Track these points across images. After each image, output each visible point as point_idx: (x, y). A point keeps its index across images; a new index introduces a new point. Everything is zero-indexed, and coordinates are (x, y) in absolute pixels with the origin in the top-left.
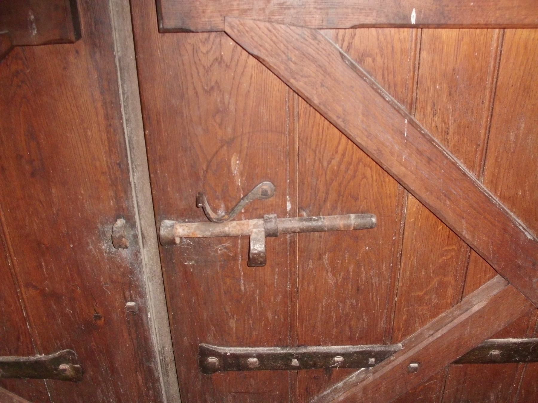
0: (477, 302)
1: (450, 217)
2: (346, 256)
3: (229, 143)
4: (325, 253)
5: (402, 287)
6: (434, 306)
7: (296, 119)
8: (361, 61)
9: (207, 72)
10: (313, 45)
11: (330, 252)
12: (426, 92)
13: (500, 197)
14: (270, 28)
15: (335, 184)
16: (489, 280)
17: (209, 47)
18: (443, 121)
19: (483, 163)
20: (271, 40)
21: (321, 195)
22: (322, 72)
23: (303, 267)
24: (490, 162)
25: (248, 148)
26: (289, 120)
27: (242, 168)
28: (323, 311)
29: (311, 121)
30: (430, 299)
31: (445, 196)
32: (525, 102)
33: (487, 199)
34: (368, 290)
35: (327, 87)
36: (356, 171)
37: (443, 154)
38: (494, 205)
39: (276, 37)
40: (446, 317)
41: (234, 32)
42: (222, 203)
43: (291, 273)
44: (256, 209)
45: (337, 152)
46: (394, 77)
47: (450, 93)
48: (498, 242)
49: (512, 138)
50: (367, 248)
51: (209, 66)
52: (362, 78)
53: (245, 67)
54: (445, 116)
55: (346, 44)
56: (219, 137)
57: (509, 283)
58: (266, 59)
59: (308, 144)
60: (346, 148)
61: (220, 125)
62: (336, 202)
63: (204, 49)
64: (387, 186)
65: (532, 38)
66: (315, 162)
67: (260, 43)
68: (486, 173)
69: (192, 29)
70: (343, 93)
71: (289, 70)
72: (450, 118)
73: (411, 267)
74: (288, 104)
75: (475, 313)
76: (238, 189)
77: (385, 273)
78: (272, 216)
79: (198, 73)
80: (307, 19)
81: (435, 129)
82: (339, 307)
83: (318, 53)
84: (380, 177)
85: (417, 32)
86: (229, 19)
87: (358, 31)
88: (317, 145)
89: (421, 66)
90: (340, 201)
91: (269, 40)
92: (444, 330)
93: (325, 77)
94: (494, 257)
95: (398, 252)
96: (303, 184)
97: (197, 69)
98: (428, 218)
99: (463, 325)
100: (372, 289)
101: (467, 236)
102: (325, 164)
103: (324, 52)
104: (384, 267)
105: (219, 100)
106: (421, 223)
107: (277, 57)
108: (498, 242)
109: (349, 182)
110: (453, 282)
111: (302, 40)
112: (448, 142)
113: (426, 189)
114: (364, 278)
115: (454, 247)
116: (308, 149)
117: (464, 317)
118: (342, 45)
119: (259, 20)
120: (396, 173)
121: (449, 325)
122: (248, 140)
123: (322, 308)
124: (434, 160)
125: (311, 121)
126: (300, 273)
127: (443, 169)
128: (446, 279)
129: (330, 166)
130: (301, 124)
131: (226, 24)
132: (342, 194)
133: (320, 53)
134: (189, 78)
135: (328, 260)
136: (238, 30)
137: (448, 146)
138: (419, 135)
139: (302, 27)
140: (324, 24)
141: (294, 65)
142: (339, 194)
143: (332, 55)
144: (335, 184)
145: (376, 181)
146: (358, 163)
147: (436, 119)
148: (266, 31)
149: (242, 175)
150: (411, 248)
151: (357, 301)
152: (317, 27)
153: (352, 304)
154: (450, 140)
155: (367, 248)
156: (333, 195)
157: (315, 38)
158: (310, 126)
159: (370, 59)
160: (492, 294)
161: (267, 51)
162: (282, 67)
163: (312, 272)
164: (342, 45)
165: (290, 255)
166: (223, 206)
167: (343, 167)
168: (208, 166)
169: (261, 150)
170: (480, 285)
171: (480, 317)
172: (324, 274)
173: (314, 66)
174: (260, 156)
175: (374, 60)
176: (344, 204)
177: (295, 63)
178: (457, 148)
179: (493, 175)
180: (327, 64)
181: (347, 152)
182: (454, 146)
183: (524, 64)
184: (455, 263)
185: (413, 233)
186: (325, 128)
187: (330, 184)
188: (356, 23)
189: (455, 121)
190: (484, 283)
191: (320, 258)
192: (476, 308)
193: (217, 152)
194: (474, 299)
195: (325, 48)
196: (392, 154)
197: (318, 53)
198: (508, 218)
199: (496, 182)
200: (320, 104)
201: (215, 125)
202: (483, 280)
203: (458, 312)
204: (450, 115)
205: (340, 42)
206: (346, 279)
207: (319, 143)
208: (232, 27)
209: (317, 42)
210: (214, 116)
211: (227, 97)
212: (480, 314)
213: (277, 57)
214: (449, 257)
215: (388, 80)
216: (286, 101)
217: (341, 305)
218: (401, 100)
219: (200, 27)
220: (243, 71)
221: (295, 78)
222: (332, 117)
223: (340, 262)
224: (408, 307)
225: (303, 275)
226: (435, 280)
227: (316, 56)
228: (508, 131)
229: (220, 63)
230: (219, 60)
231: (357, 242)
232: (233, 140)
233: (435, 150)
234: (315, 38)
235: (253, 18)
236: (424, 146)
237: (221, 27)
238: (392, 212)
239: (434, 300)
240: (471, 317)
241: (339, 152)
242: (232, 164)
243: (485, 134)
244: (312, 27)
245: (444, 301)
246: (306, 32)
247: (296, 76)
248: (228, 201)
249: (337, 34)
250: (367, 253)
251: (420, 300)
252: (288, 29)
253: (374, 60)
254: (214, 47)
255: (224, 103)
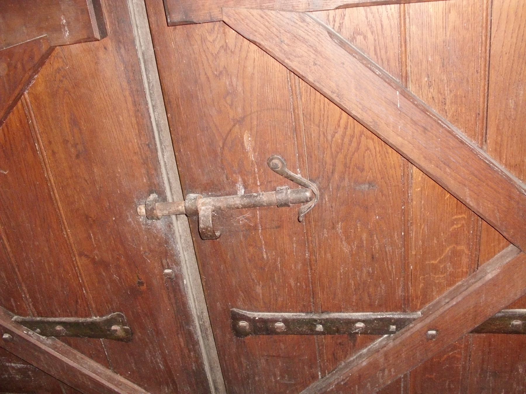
0: (491, 271)
1: (452, 184)
2: (358, 225)
3: (240, 121)
4: (338, 222)
5: (416, 255)
6: (450, 275)
7: (299, 97)
8: (353, 39)
9: (215, 58)
10: (302, 27)
11: (342, 221)
12: (420, 65)
13: (506, 165)
14: (263, 15)
15: (341, 156)
16: (503, 248)
17: (215, 37)
18: (439, 92)
19: (485, 131)
20: (265, 25)
21: (329, 167)
22: (314, 52)
23: (318, 237)
24: (492, 131)
25: (257, 125)
26: (293, 98)
27: (254, 145)
28: (341, 278)
29: (312, 98)
30: (445, 267)
31: (444, 164)
32: (522, 69)
33: (489, 166)
34: (383, 258)
35: (319, 65)
36: (359, 143)
37: (438, 123)
38: (496, 172)
39: (268, 22)
40: (462, 285)
41: (231, 20)
42: (240, 177)
43: (308, 242)
44: (270, 182)
45: (339, 126)
46: (386, 52)
47: (443, 64)
48: (504, 209)
49: (512, 105)
50: (377, 217)
51: (216, 53)
52: (351, 54)
53: (248, 52)
54: (440, 87)
55: (337, 25)
56: (231, 117)
57: (521, 251)
58: (262, 43)
59: (312, 119)
60: (348, 122)
61: (231, 105)
62: (344, 173)
63: (210, 39)
64: (390, 156)
65: (522, 5)
66: (320, 136)
67: (254, 29)
68: (488, 141)
69: (195, 21)
70: (335, 70)
71: (283, 51)
72: (446, 88)
73: (422, 236)
74: (290, 83)
75: (488, 281)
76: (252, 164)
77: (397, 241)
78: (284, 187)
79: (208, 60)
80: (294, 3)
81: (431, 100)
82: (356, 274)
83: (308, 35)
84: (382, 148)
85: (400, 8)
86: (225, 9)
87: (348, 10)
88: (320, 120)
89: (411, 40)
90: (347, 173)
91: (262, 26)
92: (460, 298)
93: (316, 55)
94: (501, 224)
95: (408, 221)
96: (311, 157)
97: (206, 56)
98: (434, 187)
99: (478, 292)
100: (387, 257)
101: (471, 204)
102: (329, 138)
103: (313, 33)
104: (396, 236)
105: (228, 83)
106: (428, 192)
107: (271, 40)
108: (504, 209)
109: (354, 154)
110: (466, 251)
111: (292, 23)
112: (446, 112)
113: (425, 157)
114: (377, 247)
115: (464, 215)
116: (312, 124)
117: (478, 285)
118: (334, 25)
119: (252, 8)
120: (393, 143)
121: (463, 293)
122: (257, 118)
123: (341, 275)
124: (429, 129)
125: (312, 98)
126: (317, 241)
127: (440, 138)
128: (458, 248)
129: (334, 139)
130: (303, 101)
131: (224, 14)
132: (348, 165)
133: (309, 34)
134: (200, 65)
135: (341, 228)
136: (235, 19)
137: (447, 116)
138: (412, 105)
139: (291, 11)
140: (311, 7)
141: (286, 47)
142: (345, 165)
143: (321, 35)
144: (341, 156)
145: (379, 152)
146: (361, 136)
147: (432, 90)
148: (259, 17)
149: (254, 150)
150: (420, 217)
151: (373, 269)
152: (304, 10)
153: (368, 272)
154: (448, 111)
155: (377, 217)
156: (339, 167)
157: (303, 21)
158: (312, 102)
159: (362, 37)
160: (505, 262)
161: (262, 35)
162: (277, 49)
163: (327, 240)
164: (334, 25)
165: (306, 225)
166: (240, 179)
167: (346, 140)
168: (224, 144)
169: (269, 128)
170: (495, 254)
171: (495, 285)
172: (339, 243)
173: (305, 46)
174: (269, 132)
175: (365, 38)
176: (351, 175)
177: (288, 45)
178: (456, 118)
179: (496, 143)
180: (317, 44)
181: (349, 126)
182: (453, 116)
183: (517, 31)
184: (466, 232)
185: (421, 202)
186: (326, 104)
187: (336, 157)
188: (340, 4)
189: (451, 91)
190: (499, 252)
191: (334, 228)
192: (489, 276)
193: (230, 131)
194: (488, 268)
195: (314, 29)
196: (387, 125)
197: (308, 35)
198: (512, 184)
199: (500, 151)
200: (314, 81)
201: (227, 105)
202: (497, 249)
203: (473, 280)
204: (446, 86)
205: (332, 23)
206: (360, 247)
207: (322, 119)
208: (228, 16)
209: (306, 24)
210: (225, 98)
211: (234, 80)
212: (494, 282)
213: (271, 40)
214: (459, 226)
215: (381, 56)
216: (288, 80)
217: (358, 273)
218: (395, 74)
219: (201, 19)
220: (247, 56)
221: (289, 59)
222: (327, 93)
223: (352, 231)
224: (424, 276)
225: (320, 244)
226: (448, 249)
227: (307, 37)
228: (507, 99)
229: (225, 50)
230: (225, 47)
231: (367, 212)
232: (243, 119)
233: (429, 119)
234: (303, 21)
235: (246, 6)
236: (418, 116)
237: (220, 17)
238: (398, 182)
239: (449, 268)
240: (484, 285)
241: (341, 126)
242: (245, 141)
243: (484, 103)
244: (300, 11)
245: (460, 270)
246: (295, 17)
247: (290, 56)
248: (244, 174)
249: (328, 16)
250: (378, 223)
251: (435, 268)
252: (279, 14)
253: (365, 38)
254: (219, 36)
255: (232, 86)
